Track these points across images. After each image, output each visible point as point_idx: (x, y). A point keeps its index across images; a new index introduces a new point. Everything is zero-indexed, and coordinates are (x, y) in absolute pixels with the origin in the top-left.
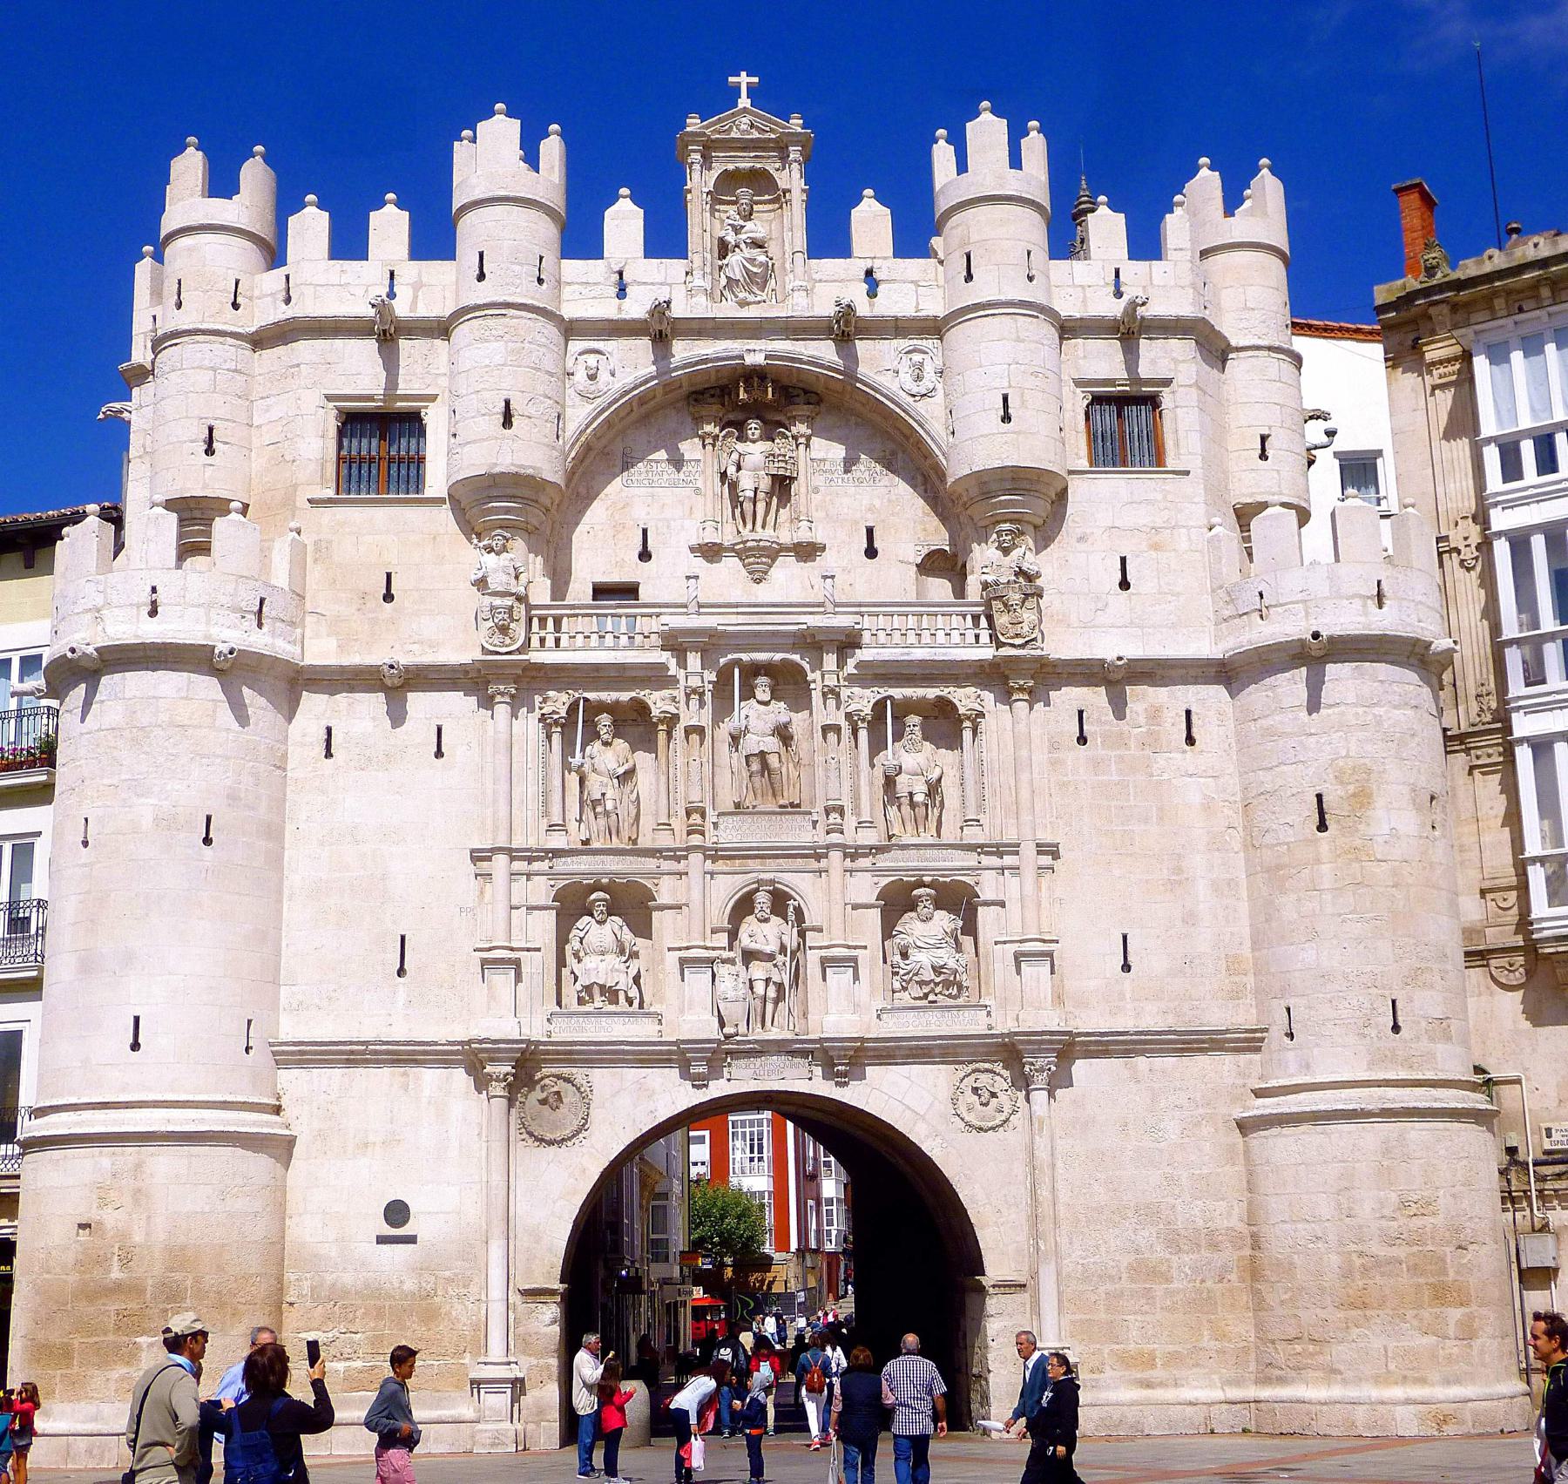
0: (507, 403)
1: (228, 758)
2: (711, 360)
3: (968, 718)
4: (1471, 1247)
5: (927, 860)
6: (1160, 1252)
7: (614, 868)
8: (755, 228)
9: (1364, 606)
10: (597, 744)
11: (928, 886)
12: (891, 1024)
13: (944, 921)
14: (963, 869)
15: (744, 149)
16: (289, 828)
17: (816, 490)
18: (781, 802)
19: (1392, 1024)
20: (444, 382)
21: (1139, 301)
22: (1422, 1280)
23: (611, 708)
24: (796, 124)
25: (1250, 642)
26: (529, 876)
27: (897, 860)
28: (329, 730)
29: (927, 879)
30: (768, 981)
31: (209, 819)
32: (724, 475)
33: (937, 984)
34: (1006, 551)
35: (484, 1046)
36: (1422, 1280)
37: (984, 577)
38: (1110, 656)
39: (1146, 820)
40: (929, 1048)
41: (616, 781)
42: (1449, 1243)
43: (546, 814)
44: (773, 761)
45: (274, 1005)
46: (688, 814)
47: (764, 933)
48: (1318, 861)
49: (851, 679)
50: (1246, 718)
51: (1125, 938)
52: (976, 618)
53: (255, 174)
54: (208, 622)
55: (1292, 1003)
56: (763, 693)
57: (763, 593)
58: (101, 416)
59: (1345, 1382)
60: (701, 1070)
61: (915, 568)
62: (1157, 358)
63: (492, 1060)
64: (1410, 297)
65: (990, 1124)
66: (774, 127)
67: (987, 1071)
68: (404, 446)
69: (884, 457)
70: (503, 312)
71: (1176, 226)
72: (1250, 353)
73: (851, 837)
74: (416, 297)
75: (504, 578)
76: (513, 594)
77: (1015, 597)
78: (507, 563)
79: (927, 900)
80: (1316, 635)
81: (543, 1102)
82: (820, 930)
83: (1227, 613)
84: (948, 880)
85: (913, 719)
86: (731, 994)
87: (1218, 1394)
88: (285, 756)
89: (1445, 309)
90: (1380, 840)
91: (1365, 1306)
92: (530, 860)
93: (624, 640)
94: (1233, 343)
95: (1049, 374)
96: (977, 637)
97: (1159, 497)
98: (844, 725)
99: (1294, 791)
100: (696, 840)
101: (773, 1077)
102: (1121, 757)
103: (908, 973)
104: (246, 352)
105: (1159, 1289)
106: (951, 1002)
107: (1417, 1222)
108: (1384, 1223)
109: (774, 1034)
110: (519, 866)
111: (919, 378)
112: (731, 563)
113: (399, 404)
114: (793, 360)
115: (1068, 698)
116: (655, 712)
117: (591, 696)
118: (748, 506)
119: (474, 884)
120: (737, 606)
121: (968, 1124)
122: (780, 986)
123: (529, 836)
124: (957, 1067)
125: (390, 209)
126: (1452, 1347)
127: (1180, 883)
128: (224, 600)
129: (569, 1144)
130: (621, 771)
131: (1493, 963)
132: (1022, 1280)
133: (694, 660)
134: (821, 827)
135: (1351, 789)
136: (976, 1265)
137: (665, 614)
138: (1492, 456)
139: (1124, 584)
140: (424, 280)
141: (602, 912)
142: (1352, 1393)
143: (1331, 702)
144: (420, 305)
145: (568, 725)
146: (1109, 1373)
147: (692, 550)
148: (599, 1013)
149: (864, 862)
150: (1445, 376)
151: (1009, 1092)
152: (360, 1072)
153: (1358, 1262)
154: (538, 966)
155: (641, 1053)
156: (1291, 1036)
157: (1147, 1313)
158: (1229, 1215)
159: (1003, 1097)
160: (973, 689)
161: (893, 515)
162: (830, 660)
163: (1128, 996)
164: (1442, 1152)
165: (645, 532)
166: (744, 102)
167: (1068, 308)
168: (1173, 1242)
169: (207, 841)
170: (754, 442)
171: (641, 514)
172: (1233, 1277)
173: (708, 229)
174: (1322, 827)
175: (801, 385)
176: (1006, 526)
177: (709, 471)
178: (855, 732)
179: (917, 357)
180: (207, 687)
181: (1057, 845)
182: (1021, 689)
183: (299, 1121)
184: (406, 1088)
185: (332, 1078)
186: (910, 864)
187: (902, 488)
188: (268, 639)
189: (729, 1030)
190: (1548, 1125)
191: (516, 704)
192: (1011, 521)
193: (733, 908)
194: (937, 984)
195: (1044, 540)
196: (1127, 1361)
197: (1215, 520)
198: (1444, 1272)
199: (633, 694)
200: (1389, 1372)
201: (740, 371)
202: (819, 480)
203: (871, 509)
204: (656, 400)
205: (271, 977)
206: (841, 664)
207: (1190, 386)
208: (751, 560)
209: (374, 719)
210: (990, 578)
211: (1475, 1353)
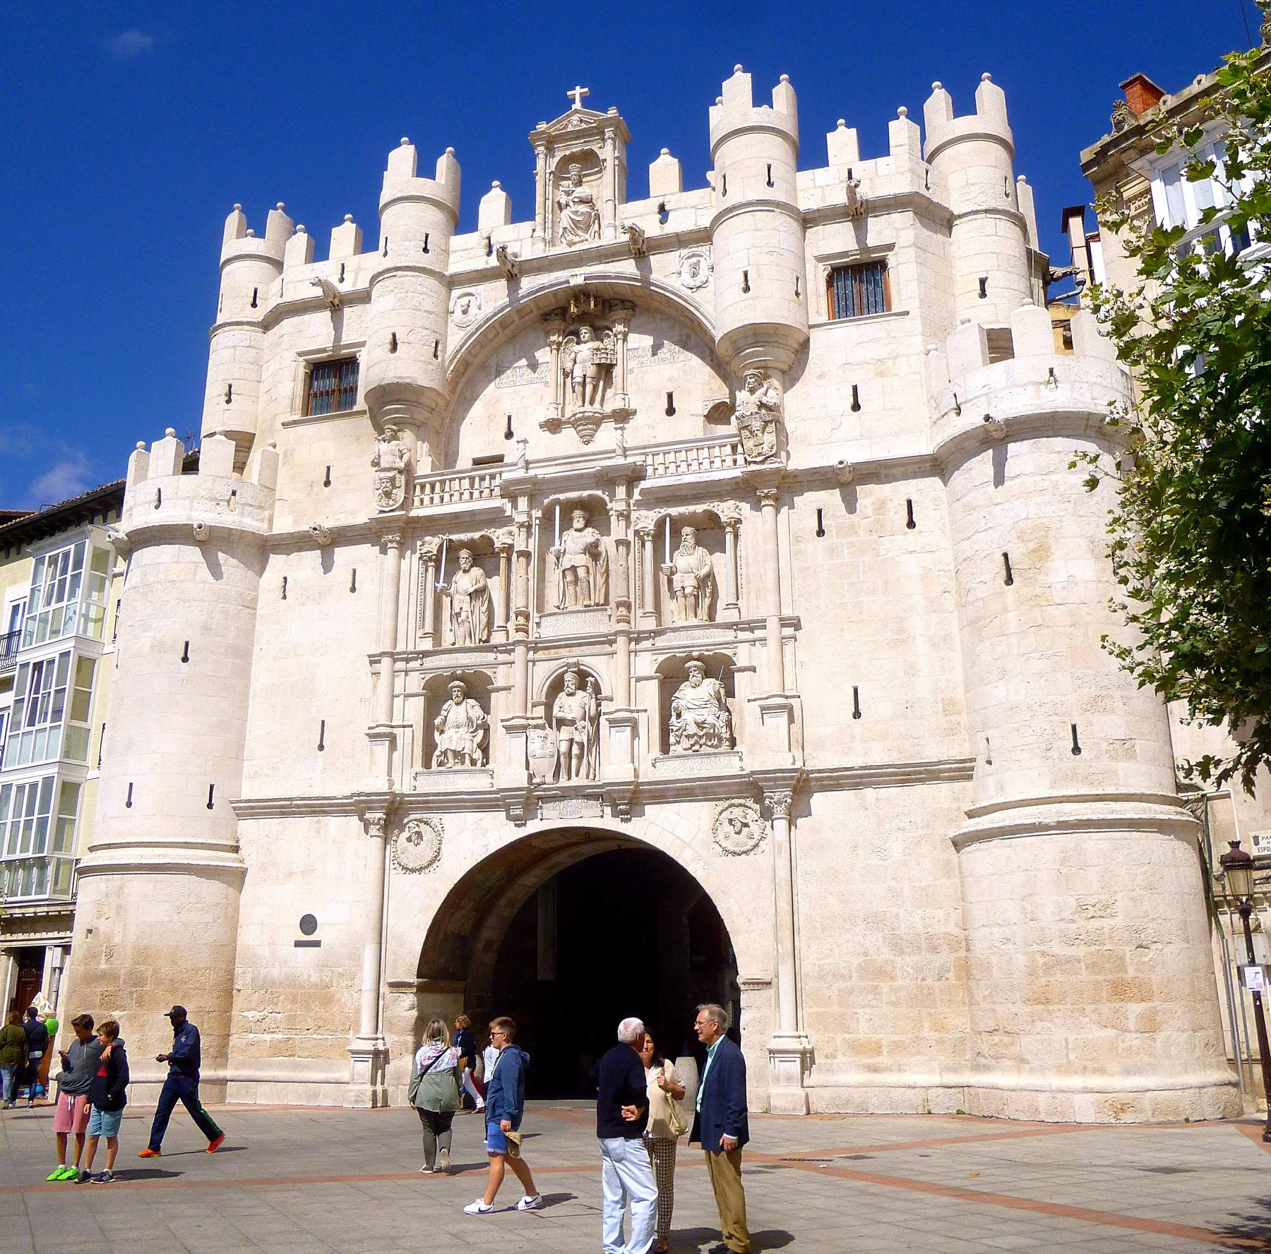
0: (394, 335)
1: (204, 601)
2: (547, 288)
3: (729, 524)
4: (1153, 946)
5: (694, 638)
6: (886, 954)
9: (1038, 390)
11: (697, 660)
12: (663, 771)
13: (710, 686)
14: (723, 644)
15: (576, 138)
16: (256, 649)
17: (632, 371)
19: (1072, 746)
22: (1100, 977)
23: (470, 545)
26: (407, 672)
27: (669, 640)
30: (571, 741)
31: (187, 644)
33: (701, 737)
35: (362, 798)
36: (1100, 977)
40: (692, 788)
41: (468, 597)
42: (1128, 943)
44: (581, 572)
45: (238, 773)
47: (571, 705)
48: (1005, 610)
49: (639, 504)
54: (191, 509)
55: (990, 733)
56: (578, 522)
57: (590, 448)
59: (1031, 1070)
60: (518, 812)
61: (702, 419)
62: (880, 230)
63: (369, 809)
64: (1105, 148)
65: (742, 849)
67: (740, 805)
69: (681, 341)
70: (394, 274)
71: (900, 130)
72: (970, 218)
74: (356, 278)
75: (390, 458)
76: (396, 469)
77: (756, 424)
78: (394, 448)
79: (695, 671)
82: (611, 700)
83: (936, 417)
84: (711, 653)
85: (687, 530)
86: (539, 752)
87: (936, 1080)
88: (255, 600)
89: (1133, 153)
90: (1059, 586)
91: (1048, 1002)
92: (407, 660)
94: (956, 213)
95: (783, 252)
96: (735, 461)
97: (884, 335)
98: (631, 537)
99: (986, 553)
101: (574, 816)
102: (852, 543)
103: (679, 729)
104: (258, 334)
105: (885, 986)
107: (1096, 923)
108: (1063, 925)
109: (575, 782)
110: (400, 665)
111: (694, 275)
112: (569, 433)
113: (343, 352)
115: (809, 501)
116: (497, 544)
117: (454, 537)
119: (370, 680)
120: (555, 460)
121: (724, 849)
122: (581, 745)
124: (717, 803)
125: (348, 224)
126: (1134, 1040)
128: (203, 493)
129: (427, 871)
130: (471, 590)
132: (767, 979)
133: (523, 503)
135: (1032, 545)
137: (505, 471)
139: (856, 407)
141: (457, 696)
142: (1037, 1081)
143: (1013, 474)
146: (841, 1058)
149: (646, 644)
150: (1140, 207)
151: (759, 822)
153: (1041, 961)
157: (874, 1007)
159: (754, 827)
160: (733, 502)
161: (687, 381)
162: (621, 491)
164: (1121, 859)
165: (509, 418)
166: (577, 105)
167: (806, 203)
168: (898, 946)
169: (185, 659)
170: (585, 343)
171: (507, 407)
172: (951, 975)
173: (551, 198)
174: (1009, 580)
175: (619, 297)
179: (694, 260)
180: (192, 554)
182: (767, 497)
183: (250, 857)
186: (681, 643)
187: (694, 361)
188: (237, 519)
190: (1254, 834)
191: (402, 547)
193: (550, 686)
194: (701, 737)
195: (790, 381)
196: (856, 1048)
198: (1122, 968)
199: (483, 533)
200: (1069, 1062)
203: (670, 379)
204: (515, 324)
205: (236, 753)
206: (629, 494)
208: (581, 428)
209: (313, 569)
211: (1158, 1044)
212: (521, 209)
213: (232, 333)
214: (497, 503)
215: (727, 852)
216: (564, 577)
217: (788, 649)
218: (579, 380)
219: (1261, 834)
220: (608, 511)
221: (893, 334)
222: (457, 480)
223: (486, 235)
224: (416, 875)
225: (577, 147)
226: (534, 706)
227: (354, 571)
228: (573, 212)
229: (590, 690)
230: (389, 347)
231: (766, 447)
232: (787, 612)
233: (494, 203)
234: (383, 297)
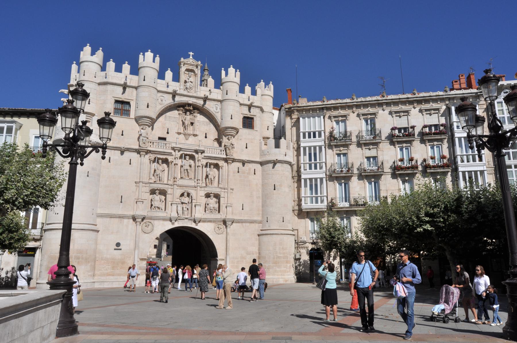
0: (148, 104)
7: (161, 187)
8: (192, 79)
13: (215, 200)
17: (197, 126)
20: (135, 97)
24: (199, 62)
29: (213, 193)
32: (182, 121)
34: (229, 140)
44: (189, 171)
46: (174, 178)
49: (203, 158)
50: (263, 171)
52: (223, 151)
53: (100, 53)
58: (60, 92)
62: (254, 112)
66: (195, 63)
68: (126, 107)
73: (200, 185)
81: (146, 226)
83: (262, 154)
91: (276, 264)
92: (146, 184)
98: (201, 166)
105: (244, 260)
107: (284, 251)
109: (187, 217)
110: (144, 185)
111: (217, 109)
112: (182, 136)
116: (169, 161)
118: (186, 127)
122: (188, 209)
123: (146, 180)
130: (163, 170)
136: (216, 256)
138: (301, 134)
139: (246, 148)
140: (132, 78)
144: (131, 83)
148: (157, 211)
149: (203, 189)
152: (112, 219)
156: (267, 222)
165: (168, 129)
166: (191, 57)
167: (242, 102)
169: (88, 176)
171: (168, 125)
174: (275, 189)
179: (217, 106)
182: (230, 163)
184: (121, 223)
189: (179, 216)
197: (261, 139)
202: (198, 124)
203: (206, 130)
210: (227, 144)
212: (176, 78)
213: (90, 84)
218: (187, 125)
219: (302, 237)
224: (146, 235)
225: (190, 68)
227: (130, 160)
229: (190, 197)
233: (169, 74)
234: (144, 93)
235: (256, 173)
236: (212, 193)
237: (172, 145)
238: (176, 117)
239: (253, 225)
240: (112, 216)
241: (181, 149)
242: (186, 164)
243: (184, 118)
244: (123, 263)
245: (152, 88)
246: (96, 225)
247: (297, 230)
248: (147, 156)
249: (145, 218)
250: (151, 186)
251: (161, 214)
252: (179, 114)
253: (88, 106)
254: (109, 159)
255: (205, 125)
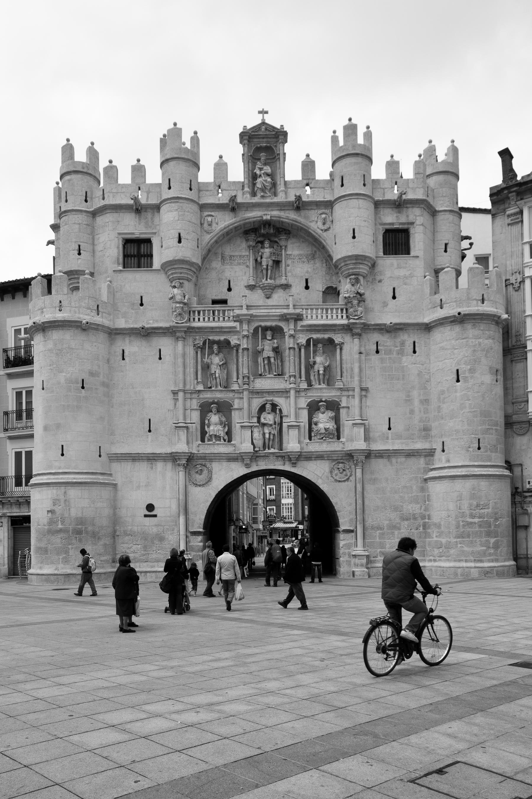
0: (179, 234)
3: (339, 344)
5: (324, 393)
6: (398, 520)
7: (219, 396)
10: (214, 355)
11: (323, 402)
17: (288, 266)
18: (275, 373)
21: (403, 193)
23: (218, 342)
25: (436, 317)
28: (123, 351)
32: (256, 260)
37: (345, 295)
38: (388, 323)
39: (398, 379)
40: (323, 455)
43: (197, 379)
44: (272, 360)
47: (268, 418)
51: (389, 419)
52: (342, 310)
65: (343, 480)
70: (177, 201)
75: (180, 297)
77: (355, 302)
80: (459, 314)
81: (197, 472)
85: (320, 345)
93: (221, 319)
96: (342, 316)
98: (296, 346)
100: (246, 387)
105: (396, 532)
106: (330, 440)
109: (272, 450)
114: (280, 217)
117: (211, 338)
119: (172, 402)
122: (274, 435)
127: (409, 400)
131: (515, 427)
132: (351, 528)
134: (288, 382)
136: (337, 524)
139: (394, 297)
145: (203, 348)
147: (246, 287)
148: (214, 444)
149: (303, 394)
154: (195, 427)
155: (228, 457)
158: (421, 509)
163: (390, 438)
172: (421, 528)
176: (353, 277)
177: (251, 259)
178: (300, 350)
179: (324, 216)
181: (368, 388)
183: (119, 479)
184: (152, 468)
185: (128, 466)
192: (355, 275)
197: (427, 274)
201: (261, 222)
207: (420, 225)
208: (266, 290)
210: (347, 295)
214: (232, 324)
215: (336, 481)
216: (264, 361)
217: (364, 400)
218: (265, 267)
220: (284, 333)
221: (411, 266)
222: (211, 312)
223: (218, 184)
224: (199, 489)
226: (252, 417)
228: (264, 180)
229: (278, 412)
230: (177, 240)
231: (359, 313)
232: (364, 385)
235: (417, 349)
236: (321, 401)
237: (235, 311)
238: (244, 254)
239: (412, 461)
240: (135, 458)
241: (252, 315)
242: (267, 348)
243: (260, 254)
244: (162, 539)
245: (185, 201)
246: (111, 475)
247: (521, 465)
248: (190, 341)
249: (193, 457)
250: (201, 396)
251: (222, 449)
252: (249, 247)
253: (78, 259)
254: (121, 352)
255: (304, 262)
